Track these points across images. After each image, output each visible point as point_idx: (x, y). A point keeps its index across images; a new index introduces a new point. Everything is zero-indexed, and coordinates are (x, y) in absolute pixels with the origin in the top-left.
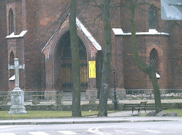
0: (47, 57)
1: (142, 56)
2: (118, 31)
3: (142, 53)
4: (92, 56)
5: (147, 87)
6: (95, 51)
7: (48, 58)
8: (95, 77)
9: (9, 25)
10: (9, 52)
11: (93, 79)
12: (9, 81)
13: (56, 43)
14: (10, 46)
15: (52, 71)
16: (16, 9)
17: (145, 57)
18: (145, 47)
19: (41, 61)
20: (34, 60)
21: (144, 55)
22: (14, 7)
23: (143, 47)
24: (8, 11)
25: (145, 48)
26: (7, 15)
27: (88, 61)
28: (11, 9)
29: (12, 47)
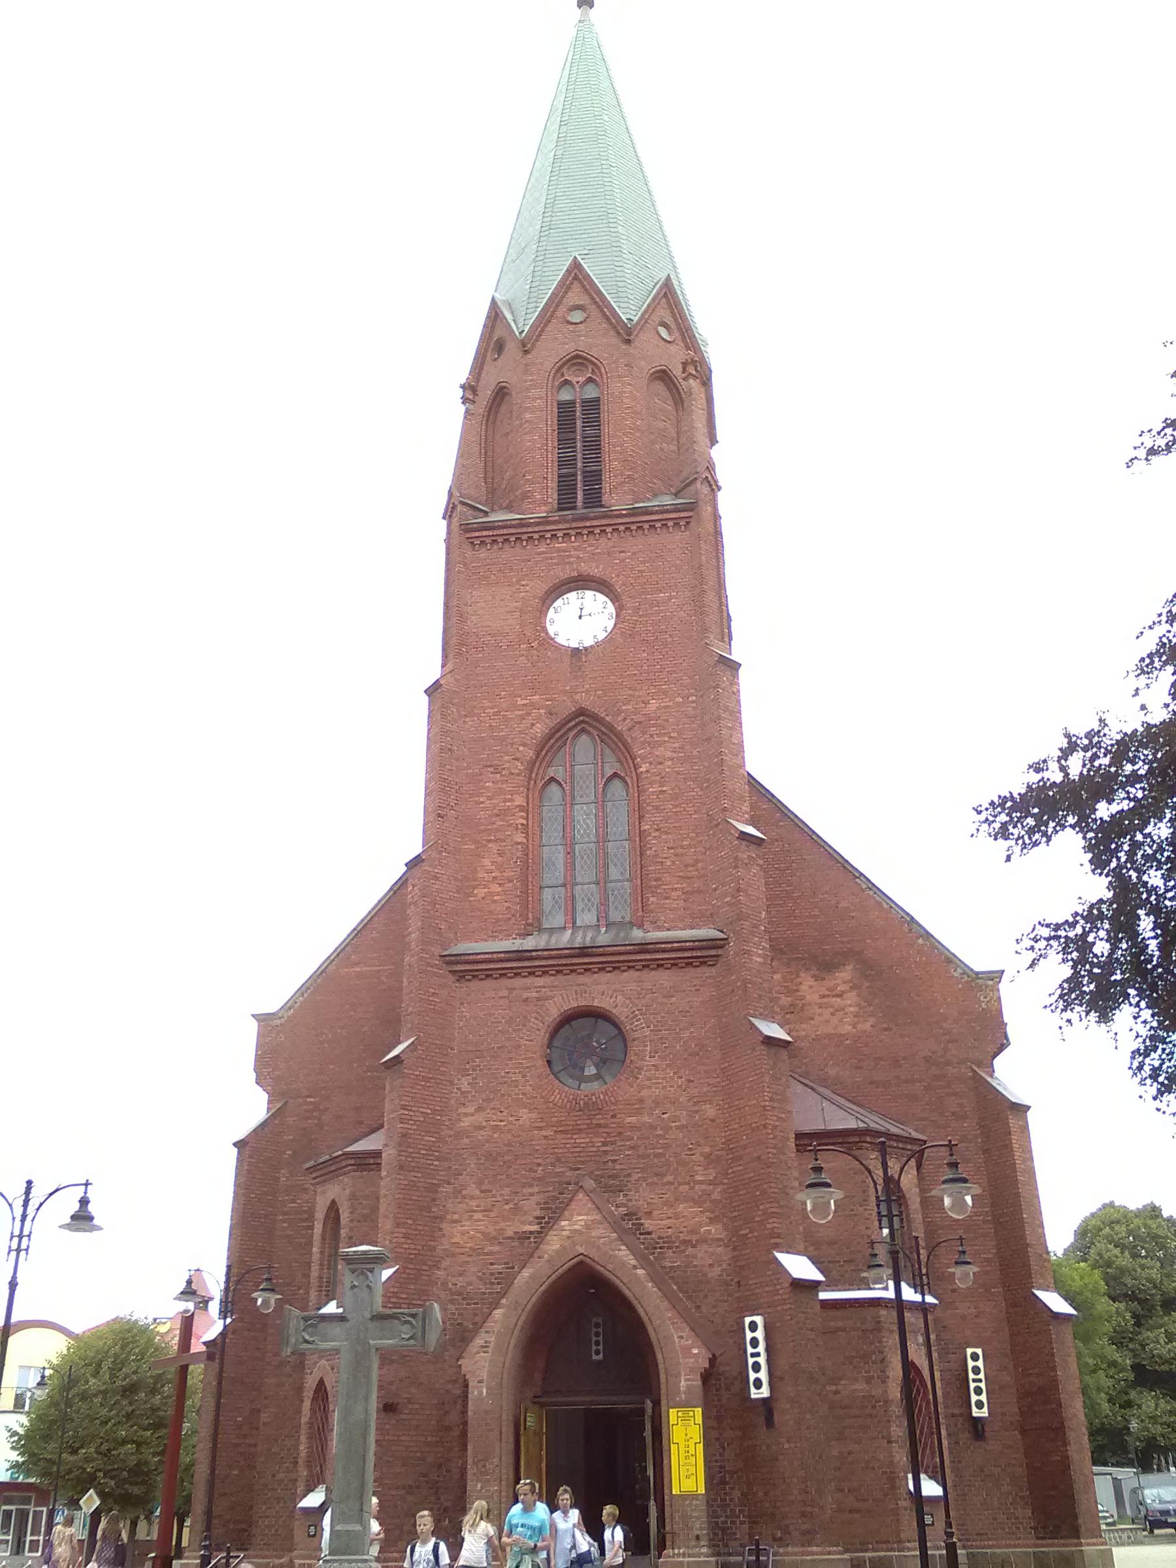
0: (479, 1391)
1: (873, 1397)
2: (800, 1267)
3: (868, 1383)
4: (683, 1383)
5: (900, 1542)
6: (696, 1361)
7: (481, 1393)
8: (702, 1490)
9: (321, 1269)
10: (311, 1382)
11: (693, 1496)
12: (298, 1515)
13: (520, 1323)
14: (315, 1357)
15: (496, 1461)
16: (353, 1197)
17: (886, 1401)
18: (880, 1357)
19: (447, 1412)
20: (417, 1406)
21: (877, 1392)
22: (348, 1191)
23: (873, 1352)
24: (320, 1214)
25: (882, 1361)
26: (318, 1228)
27: (663, 1409)
28: (333, 1202)
29: (323, 1362)
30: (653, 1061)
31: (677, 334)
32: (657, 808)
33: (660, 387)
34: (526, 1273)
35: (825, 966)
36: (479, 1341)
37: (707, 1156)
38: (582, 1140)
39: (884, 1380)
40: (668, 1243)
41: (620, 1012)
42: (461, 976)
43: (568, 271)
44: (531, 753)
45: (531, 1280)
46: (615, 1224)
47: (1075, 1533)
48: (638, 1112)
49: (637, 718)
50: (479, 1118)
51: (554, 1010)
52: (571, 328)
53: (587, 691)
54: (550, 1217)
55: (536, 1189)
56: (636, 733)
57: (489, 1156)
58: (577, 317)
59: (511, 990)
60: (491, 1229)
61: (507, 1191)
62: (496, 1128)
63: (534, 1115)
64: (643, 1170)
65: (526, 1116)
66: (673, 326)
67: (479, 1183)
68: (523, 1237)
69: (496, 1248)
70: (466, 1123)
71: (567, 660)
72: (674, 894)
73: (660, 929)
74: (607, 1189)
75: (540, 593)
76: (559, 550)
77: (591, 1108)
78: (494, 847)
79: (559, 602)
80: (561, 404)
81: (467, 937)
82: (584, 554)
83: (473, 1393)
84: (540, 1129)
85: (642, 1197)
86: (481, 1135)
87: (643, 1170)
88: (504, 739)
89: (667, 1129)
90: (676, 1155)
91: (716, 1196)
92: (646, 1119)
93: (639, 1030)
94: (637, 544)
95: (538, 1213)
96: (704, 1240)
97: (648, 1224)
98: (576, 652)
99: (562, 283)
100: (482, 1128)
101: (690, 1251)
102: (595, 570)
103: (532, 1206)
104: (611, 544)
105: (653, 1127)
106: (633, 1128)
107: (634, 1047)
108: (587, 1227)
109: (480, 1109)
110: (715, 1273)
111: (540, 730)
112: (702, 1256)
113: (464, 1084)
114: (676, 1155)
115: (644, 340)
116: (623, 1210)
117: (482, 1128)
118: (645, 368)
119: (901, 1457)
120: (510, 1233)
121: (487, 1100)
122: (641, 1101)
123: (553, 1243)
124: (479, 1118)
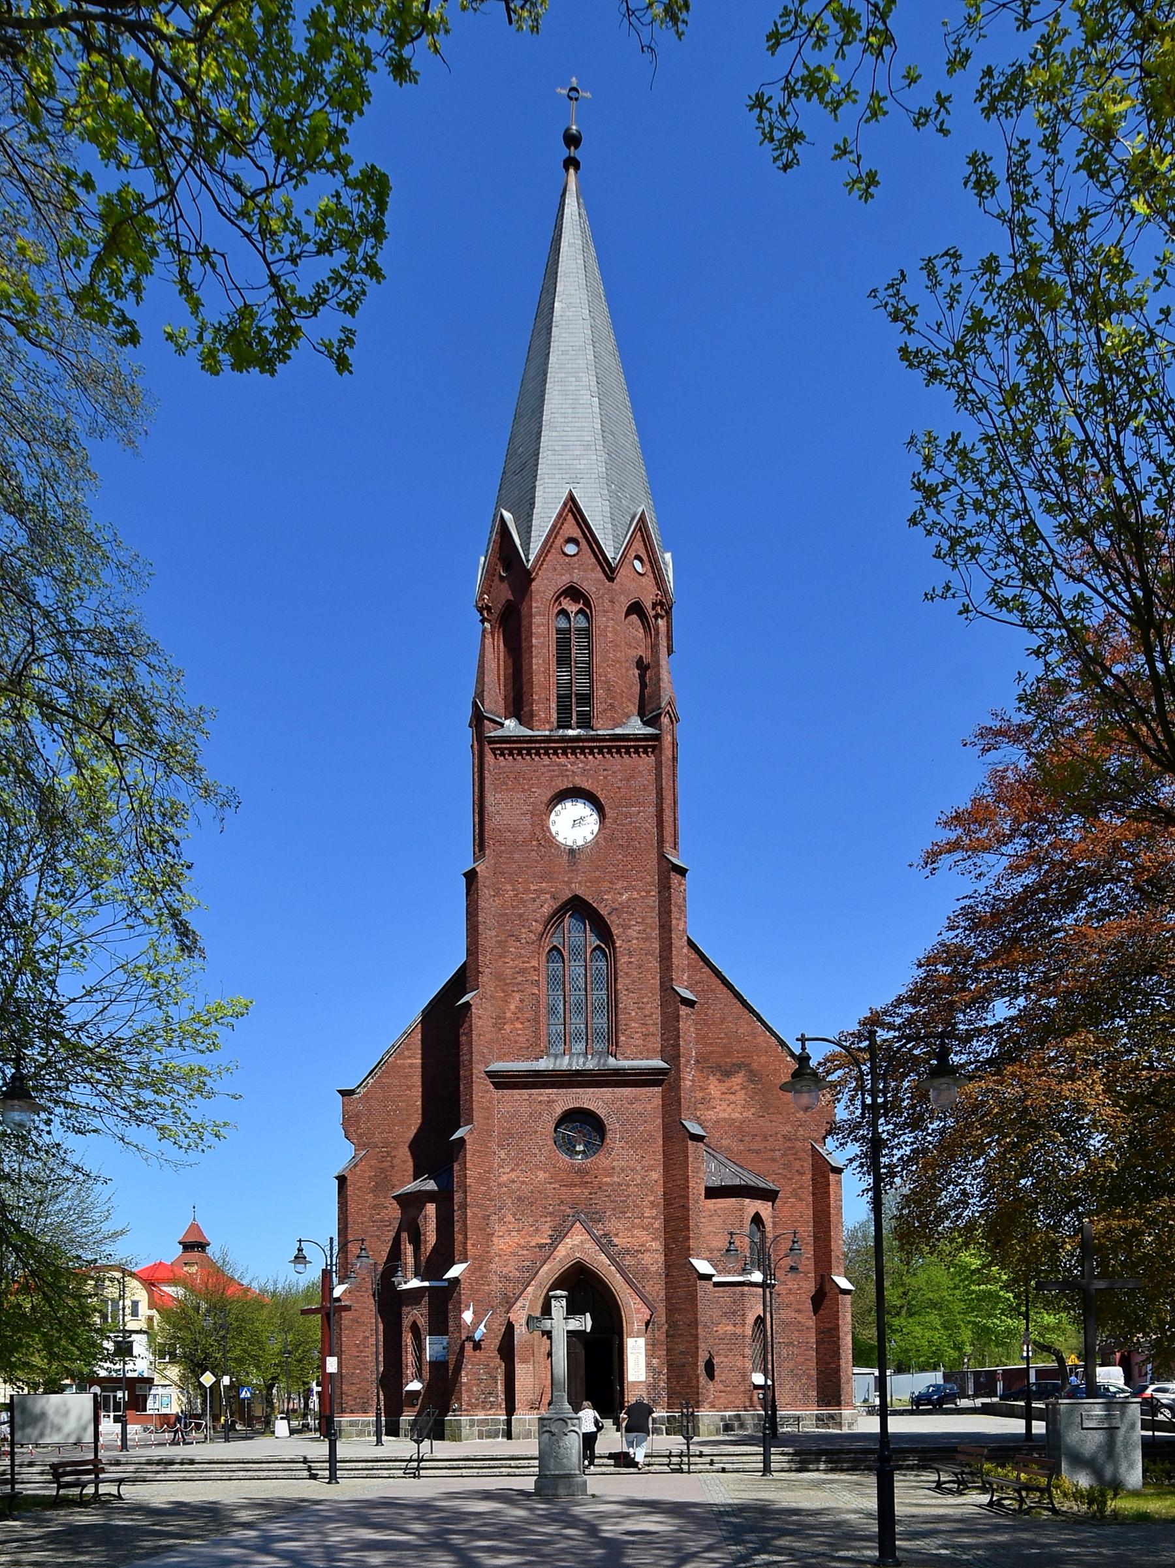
21: (739, 1331)
30: (621, 1144)
31: (648, 566)
32: (627, 973)
33: (634, 618)
34: (546, 1268)
35: (726, 1073)
36: (519, 1304)
37: (652, 1203)
38: (577, 1191)
39: (744, 1325)
40: (628, 1251)
41: (601, 1113)
42: (498, 1086)
43: (565, 504)
44: (541, 928)
45: (549, 1271)
46: (597, 1240)
47: (839, 1404)
48: (611, 1175)
49: (616, 905)
50: (513, 1175)
51: (559, 1111)
52: (567, 560)
53: (580, 883)
54: (559, 1235)
55: (549, 1219)
56: (614, 918)
57: (519, 1199)
58: (571, 549)
59: (530, 1095)
60: (522, 1242)
61: (531, 1219)
62: (523, 1182)
63: (547, 1175)
64: (614, 1209)
65: (541, 1175)
66: (645, 558)
67: (514, 1215)
68: (541, 1246)
69: (525, 1252)
70: (504, 1178)
71: (566, 857)
72: (637, 1036)
73: (627, 1058)
74: (592, 1220)
75: (545, 799)
76: (559, 765)
77: (582, 1172)
78: (517, 996)
79: (559, 807)
80: (559, 631)
81: (499, 1059)
82: (577, 769)
83: (517, 1332)
84: (550, 1183)
85: (613, 1225)
86: (514, 1186)
87: (614, 1209)
88: (521, 915)
89: (628, 1186)
90: (634, 1202)
91: (656, 1225)
92: (616, 1179)
93: (612, 1124)
94: (617, 763)
95: (550, 1233)
96: (647, 1250)
97: (616, 1240)
98: (572, 851)
99: (560, 515)
100: (514, 1182)
101: (640, 1256)
102: (586, 785)
103: (546, 1229)
104: (597, 762)
105: (620, 1185)
106: (608, 1184)
107: (609, 1135)
108: (582, 1242)
109: (513, 1170)
110: (653, 1269)
111: (546, 910)
112: (647, 1259)
113: (503, 1155)
114: (634, 1202)
115: (623, 574)
116: (601, 1232)
117: (514, 1182)
118: (624, 603)
119: (749, 1365)
120: (533, 1244)
121: (517, 1165)
122: (613, 1168)
123: (562, 1251)
124: (513, 1175)
